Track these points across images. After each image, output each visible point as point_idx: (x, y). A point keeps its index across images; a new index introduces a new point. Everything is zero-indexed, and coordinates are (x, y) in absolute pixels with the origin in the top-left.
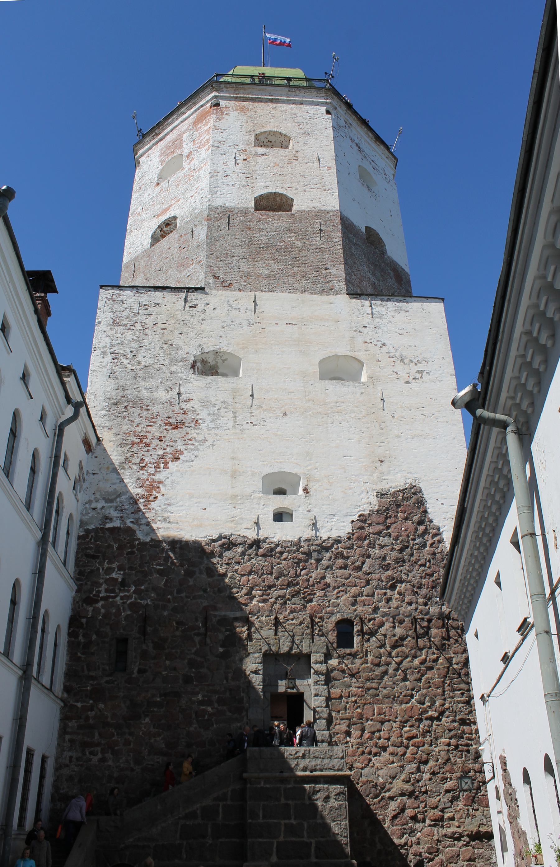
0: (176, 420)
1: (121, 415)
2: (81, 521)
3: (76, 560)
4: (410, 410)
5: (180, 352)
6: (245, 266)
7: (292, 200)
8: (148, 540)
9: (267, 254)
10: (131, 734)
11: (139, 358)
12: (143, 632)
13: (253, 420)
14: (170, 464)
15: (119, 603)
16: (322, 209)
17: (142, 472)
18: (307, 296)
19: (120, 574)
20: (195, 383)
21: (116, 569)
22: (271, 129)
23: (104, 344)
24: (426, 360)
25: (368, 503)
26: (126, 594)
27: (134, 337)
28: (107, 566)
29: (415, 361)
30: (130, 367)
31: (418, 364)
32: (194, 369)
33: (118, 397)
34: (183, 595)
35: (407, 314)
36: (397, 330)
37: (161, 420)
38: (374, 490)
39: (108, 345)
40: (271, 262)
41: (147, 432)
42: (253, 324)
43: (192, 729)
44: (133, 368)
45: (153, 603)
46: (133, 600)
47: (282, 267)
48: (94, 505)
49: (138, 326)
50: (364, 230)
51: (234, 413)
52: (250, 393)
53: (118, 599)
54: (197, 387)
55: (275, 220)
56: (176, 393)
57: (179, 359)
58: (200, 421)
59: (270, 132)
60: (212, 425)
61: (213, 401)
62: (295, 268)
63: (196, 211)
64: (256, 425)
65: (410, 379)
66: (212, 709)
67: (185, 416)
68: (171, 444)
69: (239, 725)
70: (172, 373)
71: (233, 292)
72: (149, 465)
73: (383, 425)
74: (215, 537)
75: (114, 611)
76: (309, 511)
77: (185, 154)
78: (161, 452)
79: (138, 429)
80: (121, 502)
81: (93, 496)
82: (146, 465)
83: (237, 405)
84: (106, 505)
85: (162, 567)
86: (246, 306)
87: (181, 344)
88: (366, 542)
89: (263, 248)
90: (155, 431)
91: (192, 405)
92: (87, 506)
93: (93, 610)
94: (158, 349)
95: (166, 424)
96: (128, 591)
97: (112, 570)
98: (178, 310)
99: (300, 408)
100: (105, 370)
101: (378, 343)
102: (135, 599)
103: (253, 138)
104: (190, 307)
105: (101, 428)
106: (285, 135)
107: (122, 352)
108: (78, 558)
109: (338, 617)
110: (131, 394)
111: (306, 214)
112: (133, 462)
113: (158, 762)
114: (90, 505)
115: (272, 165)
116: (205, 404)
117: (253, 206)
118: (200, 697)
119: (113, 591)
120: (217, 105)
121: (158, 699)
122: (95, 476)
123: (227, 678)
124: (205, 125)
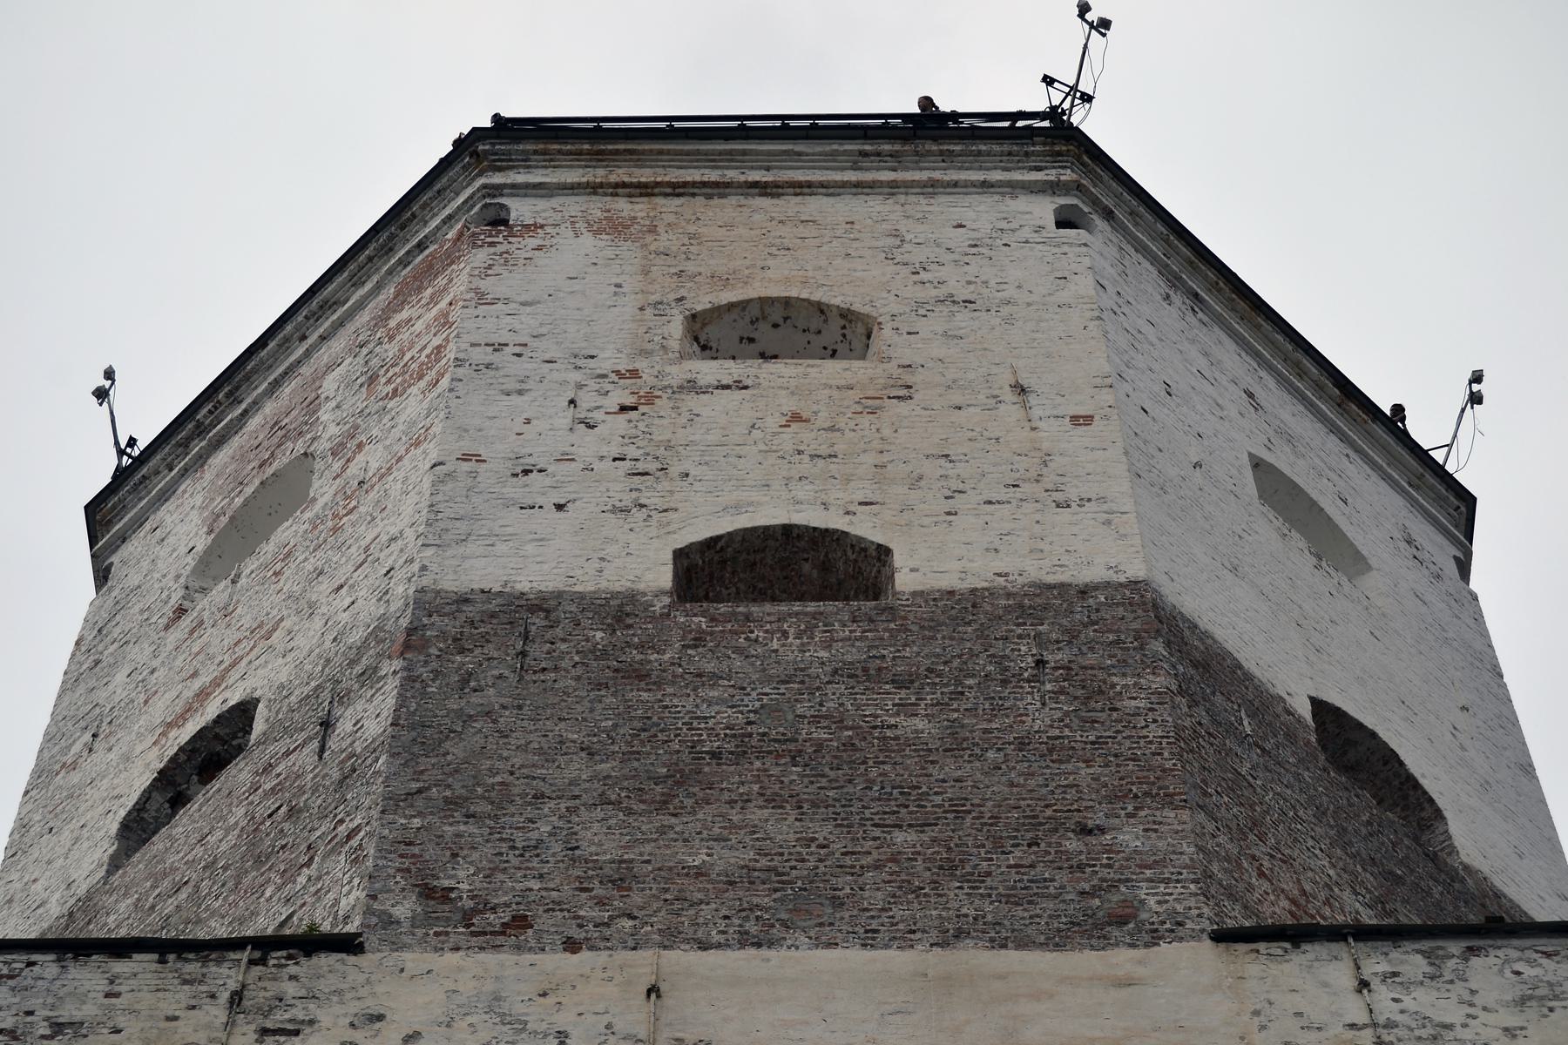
6: (601, 839)
7: (884, 552)
16: (1051, 579)
18: (974, 958)
40: (757, 814)
47: (823, 832)
50: (1305, 710)
55: (791, 640)
59: (765, 302)
62: (899, 837)
63: (356, 637)
71: (529, 957)
77: (322, 446)
86: (606, 1019)
89: (716, 755)
103: (676, 328)
104: (265, 1032)
106: (847, 315)
111: (962, 608)
115: (773, 422)
117: (663, 577)
120: (499, 221)
124: (434, 300)
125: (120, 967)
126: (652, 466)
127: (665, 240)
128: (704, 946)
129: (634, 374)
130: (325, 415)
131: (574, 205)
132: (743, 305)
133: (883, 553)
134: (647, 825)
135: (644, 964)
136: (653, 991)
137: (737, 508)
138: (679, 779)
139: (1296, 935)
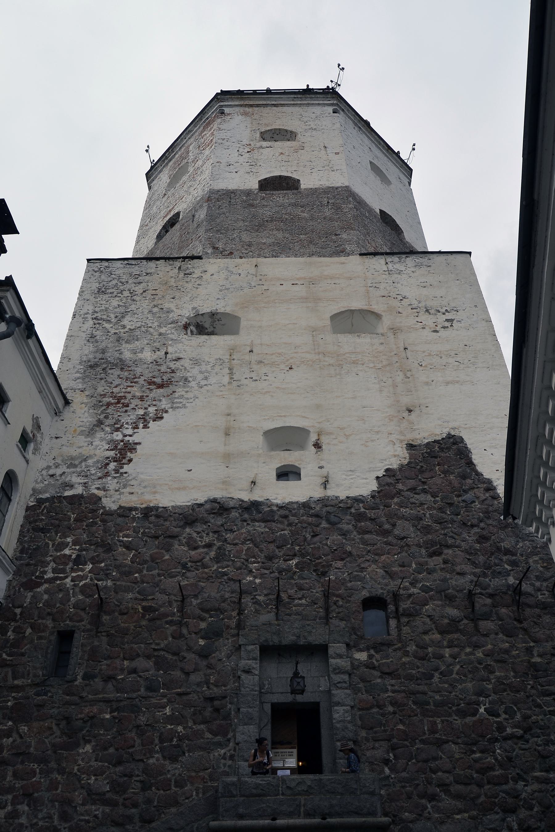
0: (163, 379)
1: (98, 377)
2: (34, 490)
3: (20, 535)
4: (441, 358)
5: (171, 315)
6: (246, 237)
7: (299, 181)
8: (114, 507)
9: (270, 226)
10: (61, 771)
11: (125, 322)
12: (96, 621)
13: (253, 375)
14: (151, 424)
15: (68, 586)
16: (331, 186)
17: (116, 433)
18: (315, 259)
19: (75, 549)
20: (186, 342)
21: (71, 544)
22: (277, 127)
23: (86, 311)
24: (455, 309)
25: (394, 456)
26: (80, 573)
27: (121, 304)
28: (60, 540)
29: (444, 310)
30: (113, 331)
31: (447, 314)
32: (186, 330)
33: (96, 360)
34: (155, 572)
35: (429, 269)
36: (419, 284)
37: (145, 380)
38: (401, 441)
39: (90, 312)
40: (275, 232)
41: (126, 392)
42: (255, 286)
43: (151, 761)
44: (117, 331)
45: (114, 584)
46: (88, 580)
47: (287, 236)
48: (51, 472)
49: (126, 293)
50: (378, 212)
51: (230, 369)
52: (249, 349)
53: (68, 580)
54: (189, 346)
55: (281, 198)
56: (164, 353)
57: (170, 321)
58: (190, 379)
60: (203, 382)
61: (207, 359)
62: (301, 236)
63: (198, 199)
64: (257, 380)
65: (438, 329)
66: (184, 728)
67: (173, 375)
68: (154, 403)
69: (223, 751)
70: (160, 334)
71: (233, 260)
72: (126, 426)
73: (409, 374)
74: (201, 500)
75: (60, 596)
76: (321, 467)
77: (190, 161)
78: (141, 412)
79: (115, 390)
80: (87, 467)
81: (53, 462)
82: (122, 426)
83: (235, 361)
84: (68, 470)
85: (130, 539)
87: (172, 306)
88: (396, 500)
90: (136, 391)
91: (182, 364)
92: (44, 472)
93: (32, 596)
94: (146, 313)
95: (150, 383)
96: (82, 570)
97: (67, 545)
98: (172, 277)
99: (308, 361)
100: (84, 335)
101: (398, 296)
102: (91, 579)
103: (258, 135)
104: (185, 274)
105: (73, 391)
106: (291, 132)
107: (105, 317)
108: (23, 532)
109: (365, 594)
110: (111, 355)
111: (314, 192)
112: (107, 424)
113: (96, 816)
114: (47, 472)
115: (277, 154)
116: (196, 362)
117: (257, 186)
118: (168, 711)
119: (63, 571)
120: (222, 113)
121: (108, 716)
122: (58, 440)
123: (207, 683)
124: (210, 130)
125: (158, 262)
126: (254, 164)
127: (256, 116)
128: (265, 257)
129: (250, 145)
130: (190, 154)
131: (237, 109)
132: (271, 130)
133: (299, 181)
134: (254, 235)
135: (254, 261)
136: (256, 266)
137: (270, 172)
138: (260, 226)
139: (375, 254)
